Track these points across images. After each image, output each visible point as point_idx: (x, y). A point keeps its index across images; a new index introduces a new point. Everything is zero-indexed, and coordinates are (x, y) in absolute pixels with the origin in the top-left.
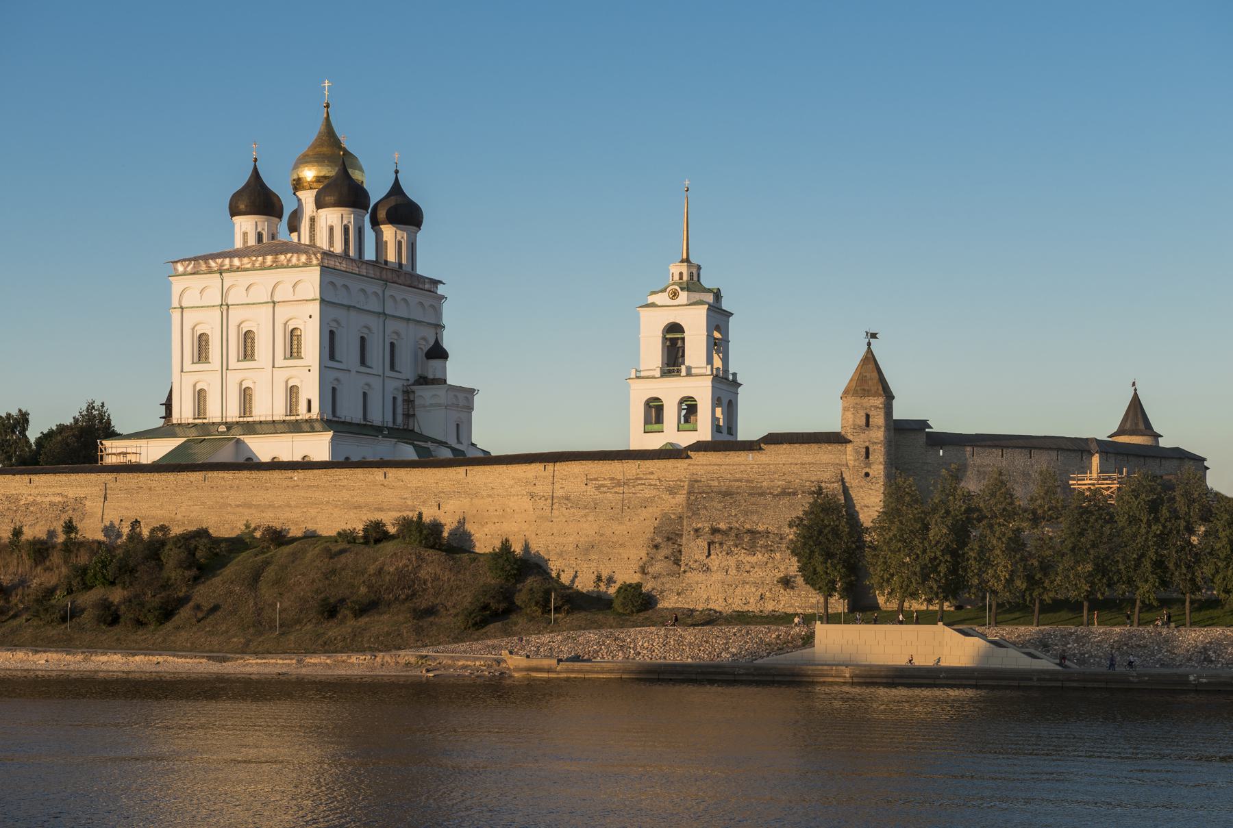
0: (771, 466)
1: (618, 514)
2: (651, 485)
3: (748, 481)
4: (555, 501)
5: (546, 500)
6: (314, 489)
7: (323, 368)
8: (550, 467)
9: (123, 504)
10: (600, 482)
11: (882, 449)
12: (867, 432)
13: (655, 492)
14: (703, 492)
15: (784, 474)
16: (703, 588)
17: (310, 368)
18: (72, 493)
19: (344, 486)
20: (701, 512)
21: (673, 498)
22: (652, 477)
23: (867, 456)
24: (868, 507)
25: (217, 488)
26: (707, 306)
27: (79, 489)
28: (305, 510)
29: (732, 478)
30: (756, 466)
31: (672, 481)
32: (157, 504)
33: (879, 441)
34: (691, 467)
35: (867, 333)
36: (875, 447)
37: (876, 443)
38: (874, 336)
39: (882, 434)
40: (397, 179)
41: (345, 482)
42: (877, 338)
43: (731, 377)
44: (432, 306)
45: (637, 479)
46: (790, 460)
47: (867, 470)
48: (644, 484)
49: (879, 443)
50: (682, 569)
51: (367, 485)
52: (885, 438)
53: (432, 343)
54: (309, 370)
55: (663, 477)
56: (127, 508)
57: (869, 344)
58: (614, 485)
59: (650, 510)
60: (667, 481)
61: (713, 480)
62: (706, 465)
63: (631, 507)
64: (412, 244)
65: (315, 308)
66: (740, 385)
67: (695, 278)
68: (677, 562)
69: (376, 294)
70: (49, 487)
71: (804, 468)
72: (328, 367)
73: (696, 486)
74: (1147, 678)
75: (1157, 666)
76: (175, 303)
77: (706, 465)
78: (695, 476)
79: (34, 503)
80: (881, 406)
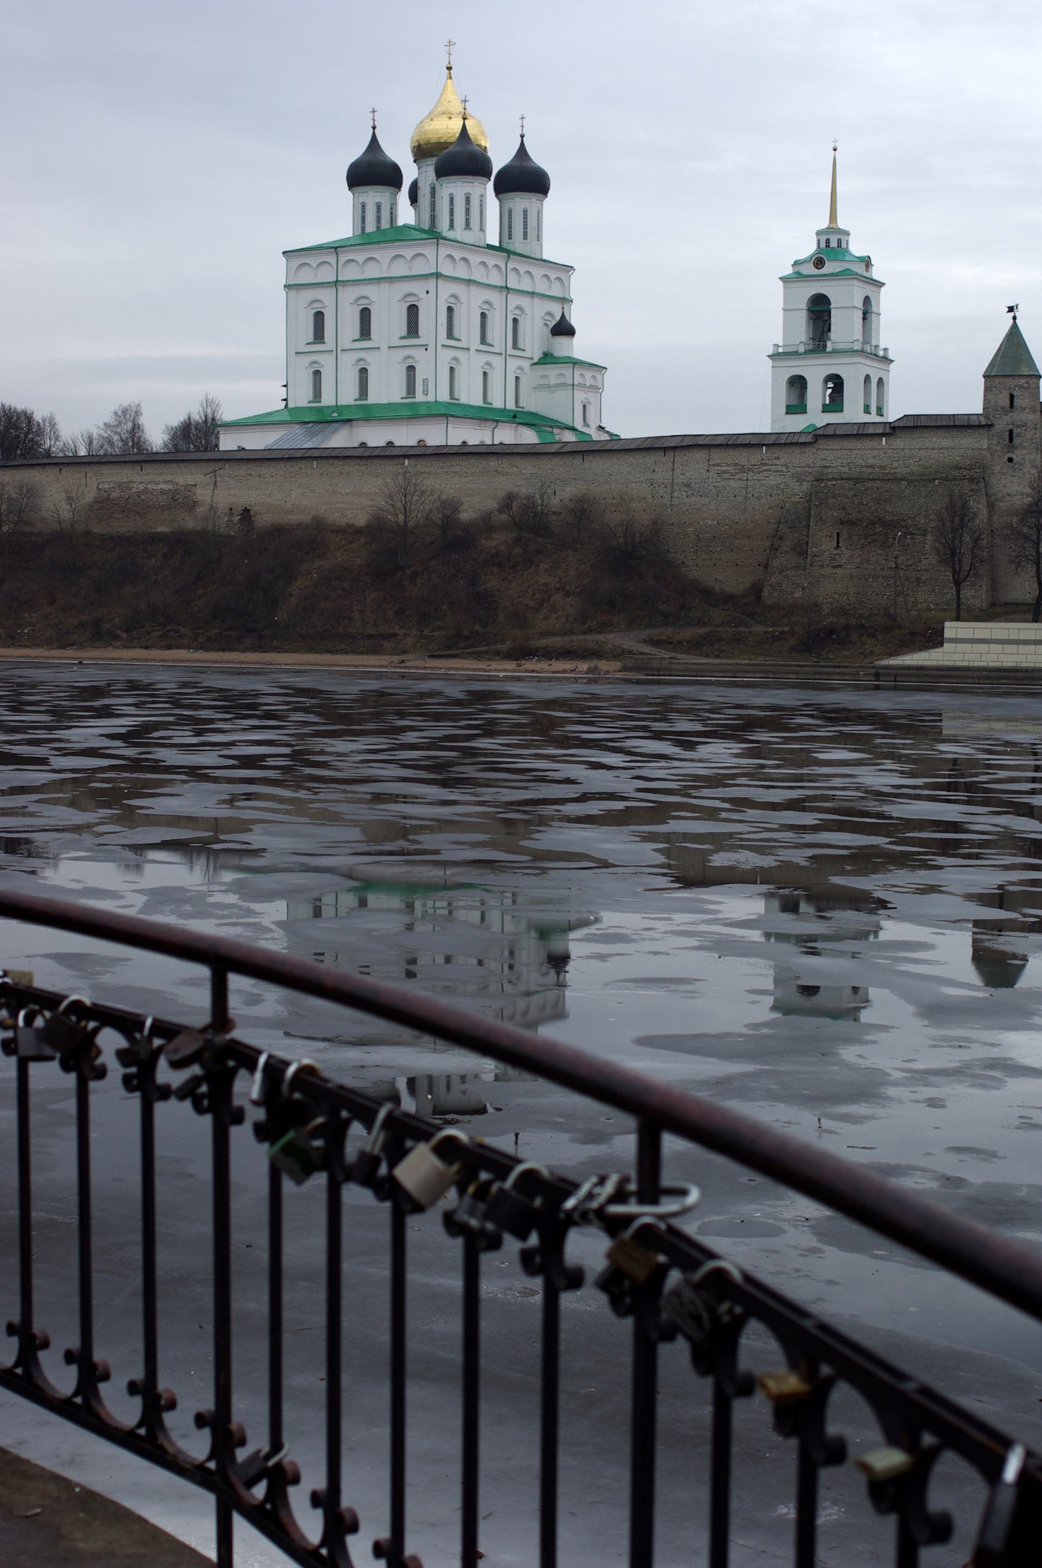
0: (906, 451)
2: (778, 471)
3: (881, 467)
4: (676, 488)
5: (666, 487)
6: (426, 476)
9: (232, 492)
10: (723, 468)
12: (1011, 414)
15: (920, 460)
19: (456, 473)
20: (831, 501)
23: (1011, 439)
24: (1009, 495)
25: (327, 474)
27: (189, 476)
29: (864, 464)
30: (890, 451)
31: (800, 467)
36: (1019, 430)
40: (522, 144)
43: (881, 353)
44: (559, 279)
46: (927, 445)
47: (1010, 455)
48: (770, 470)
49: (1023, 426)
53: (558, 317)
54: (426, 349)
58: (737, 471)
61: (844, 466)
67: (844, 245)
68: (804, 554)
69: (497, 266)
71: (941, 453)
79: (145, 491)
80: (1025, 385)
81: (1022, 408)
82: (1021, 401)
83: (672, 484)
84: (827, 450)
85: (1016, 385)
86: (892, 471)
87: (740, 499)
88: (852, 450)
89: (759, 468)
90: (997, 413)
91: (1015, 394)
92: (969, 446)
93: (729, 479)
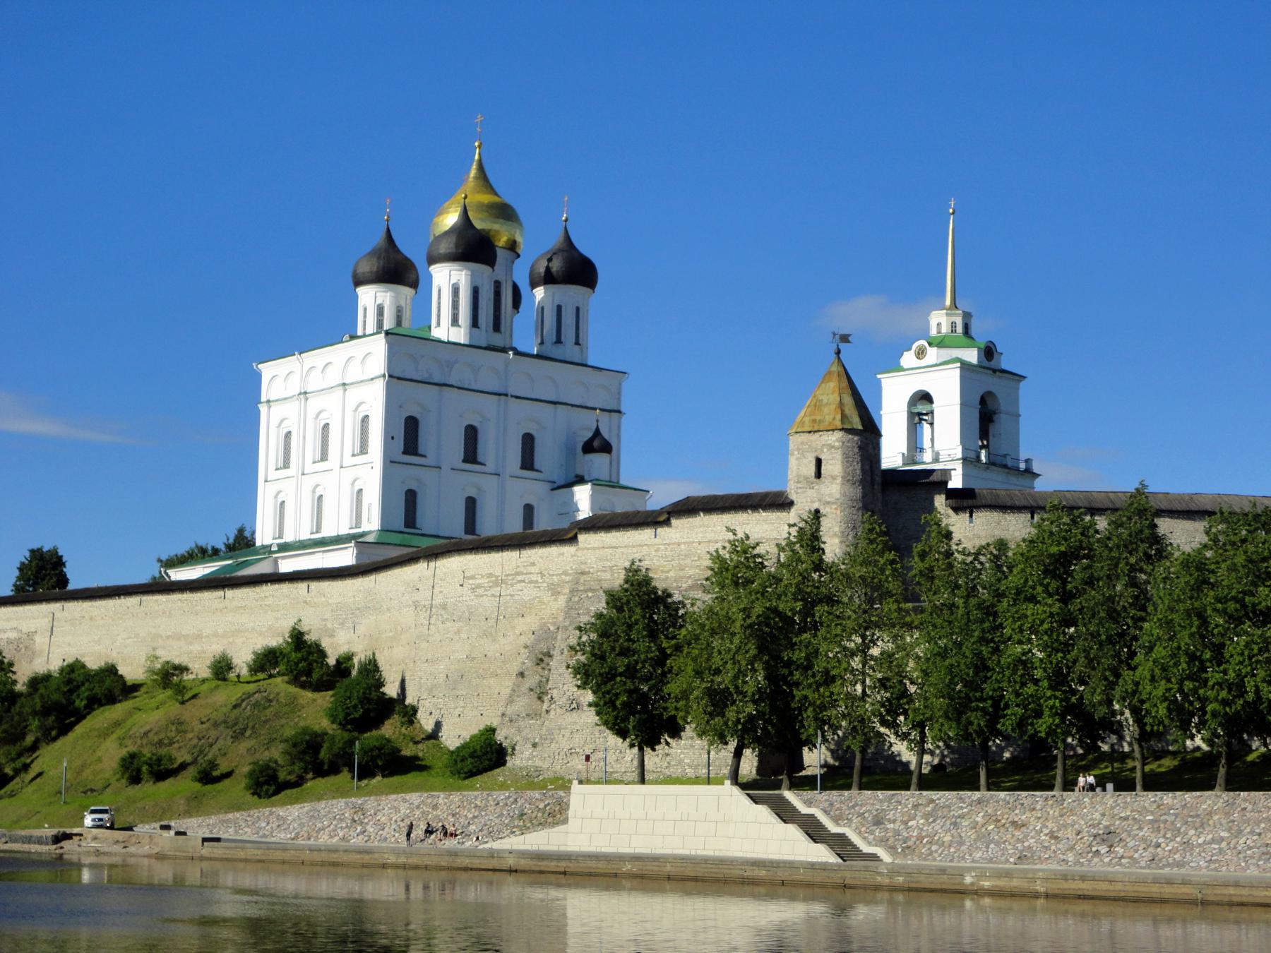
0: (683, 546)
1: (493, 626)
2: (531, 582)
4: (434, 610)
5: (426, 610)
6: (242, 611)
7: (390, 462)
8: (432, 564)
10: (477, 581)
11: (838, 512)
12: (816, 487)
13: (535, 592)
14: (590, 590)
16: (567, 735)
17: (371, 465)
18: (26, 626)
19: (269, 606)
21: (556, 600)
22: (532, 569)
26: (959, 365)
28: (231, 640)
30: (663, 547)
31: (556, 575)
32: (96, 638)
33: (832, 500)
34: (579, 553)
35: (834, 334)
37: (828, 503)
38: (845, 338)
39: (838, 487)
41: (270, 601)
42: (849, 342)
43: (1022, 466)
45: (518, 574)
48: (523, 581)
49: (833, 503)
50: (545, 707)
51: (291, 603)
52: (844, 495)
55: (546, 570)
56: (69, 645)
57: (838, 352)
58: (491, 584)
59: (528, 619)
60: (550, 575)
61: (605, 571)
62: (599, 548)
63: (507, 616)
64: (578, 309)
65: (379, 389)
66: (1037, 475)
70: (8, 620)
72: (395, 462)
73: (582, 581)
74: (901, 879)
75: (1012, 860)
76: (263, 399)
77: (599, 548)
78: (583, 567)
80: (837, 444)
81: (832, 476)
82: (831, 467)
83: (431, 607)
84: (588, 549)
85: (824, 445)
86: (663, 577)
87: (492, 622)
88: (617, 548)
89: (513, 579)
90: (799, 485)
91: (822, 457)
92: (764, 535)
93: (482, 596)
